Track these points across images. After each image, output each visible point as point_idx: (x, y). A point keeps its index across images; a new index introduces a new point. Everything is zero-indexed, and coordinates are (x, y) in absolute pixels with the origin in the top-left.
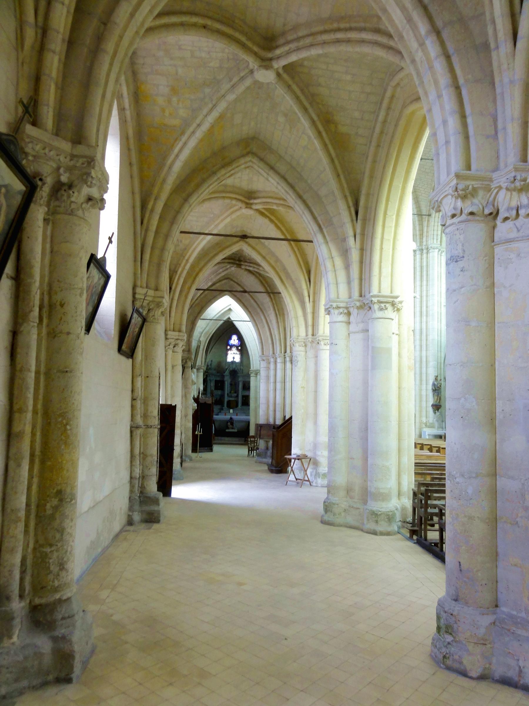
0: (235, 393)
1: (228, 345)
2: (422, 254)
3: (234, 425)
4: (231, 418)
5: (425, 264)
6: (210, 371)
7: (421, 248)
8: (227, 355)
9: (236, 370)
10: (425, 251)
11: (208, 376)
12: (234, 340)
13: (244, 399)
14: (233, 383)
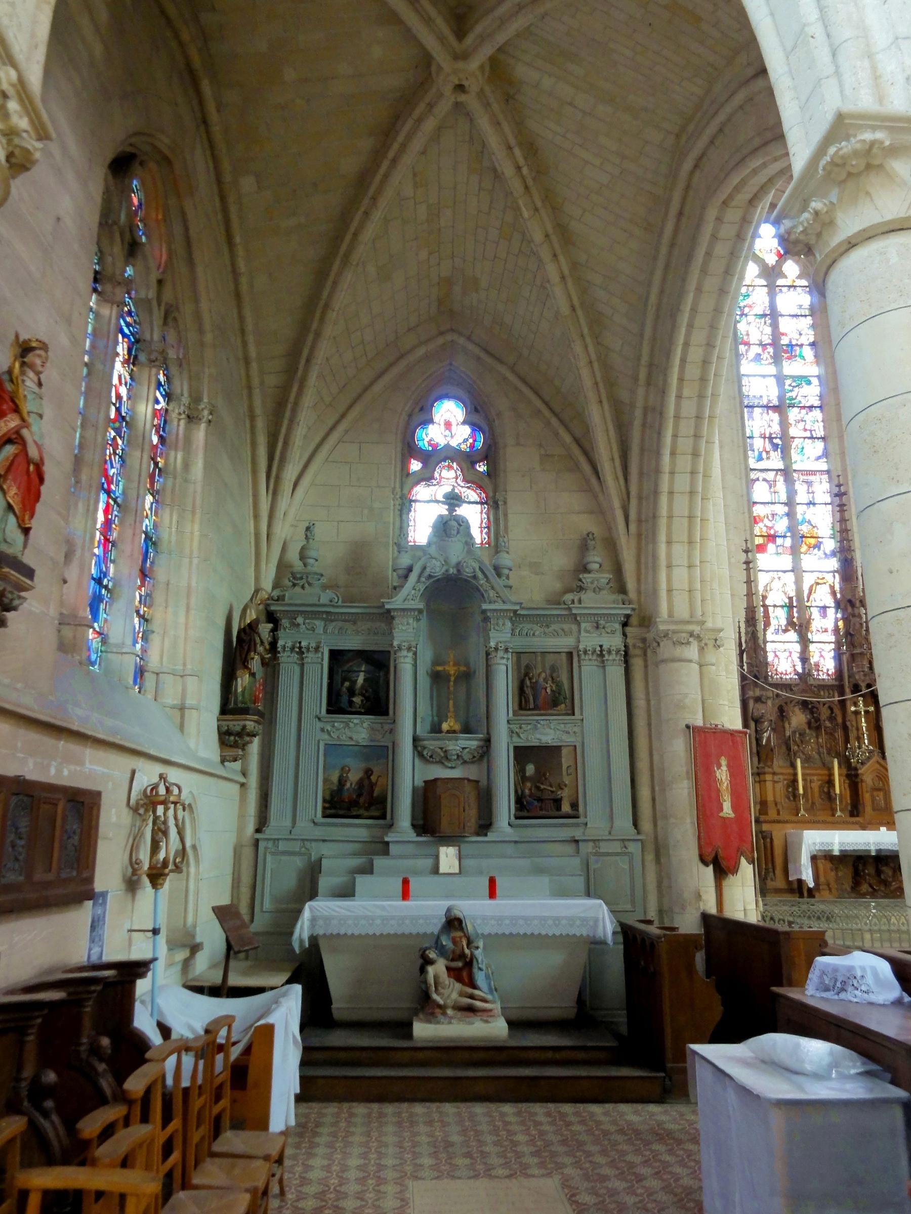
0: (467, 729)
1: (410, 449)
3: (480, 978)
4: (453, 923)
6: (296, 596)
8: (405, 504)
9: (467, 572)
11: (285, 622)
12: (448, 425)
13: (530, 769)
14: (452, 670)
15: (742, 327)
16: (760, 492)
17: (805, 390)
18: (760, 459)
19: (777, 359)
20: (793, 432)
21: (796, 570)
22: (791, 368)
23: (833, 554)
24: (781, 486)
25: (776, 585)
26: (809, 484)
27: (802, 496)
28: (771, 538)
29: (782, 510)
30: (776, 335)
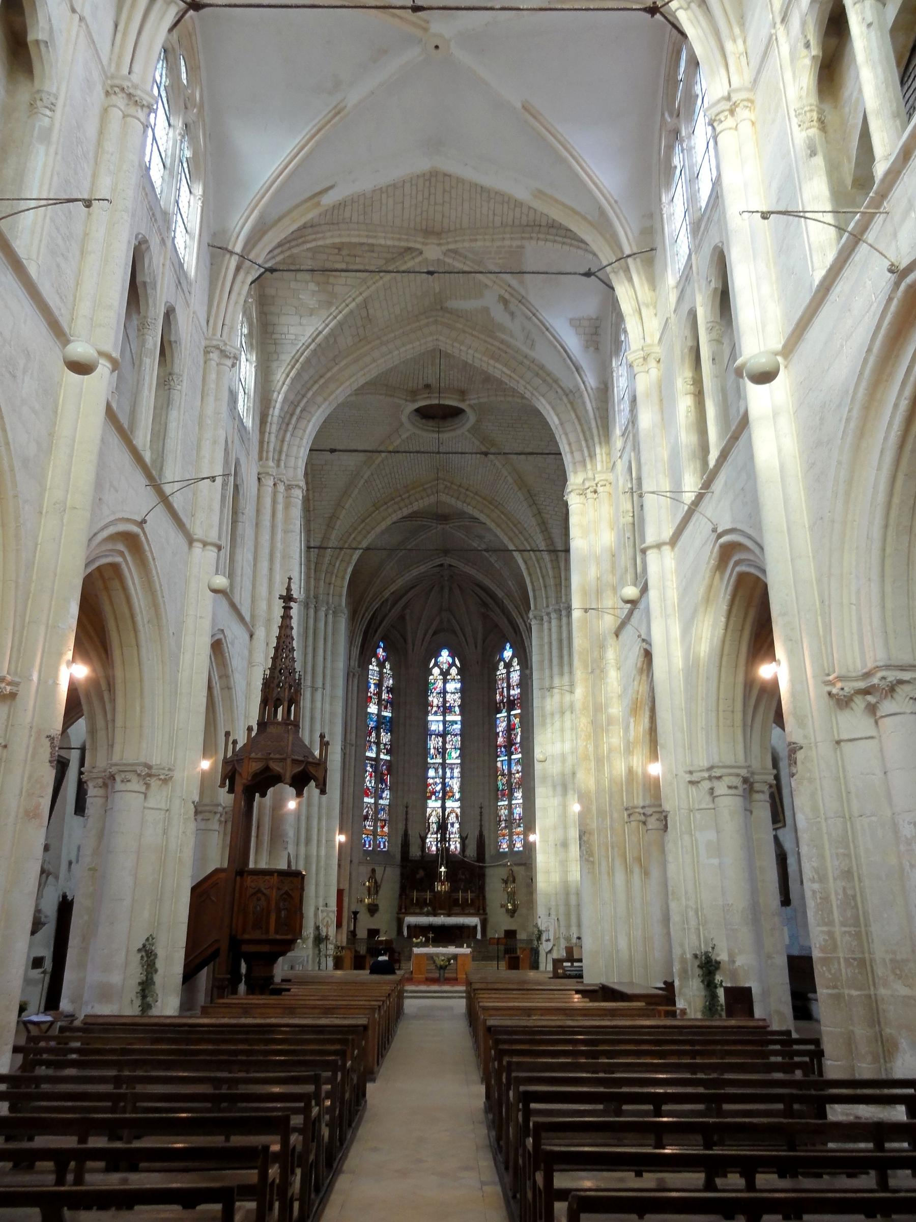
2: (560, 619)
5: (565, 635)
7: (557, 607)
10: (564, 613)
15: (430, 699)
16: (431, 773)
17: (455, 726)
18: (432, 758)
19: (444, 714)
20: (448, 746)
21: (444, 808)
22: (449, 718)
23: (459, 800)
24: (440, 771)
25: (434, 813)
26: (452, 769)
27: (448, 774)
28: (434, 793)
29: (438, 781)
30: (445, 701)
